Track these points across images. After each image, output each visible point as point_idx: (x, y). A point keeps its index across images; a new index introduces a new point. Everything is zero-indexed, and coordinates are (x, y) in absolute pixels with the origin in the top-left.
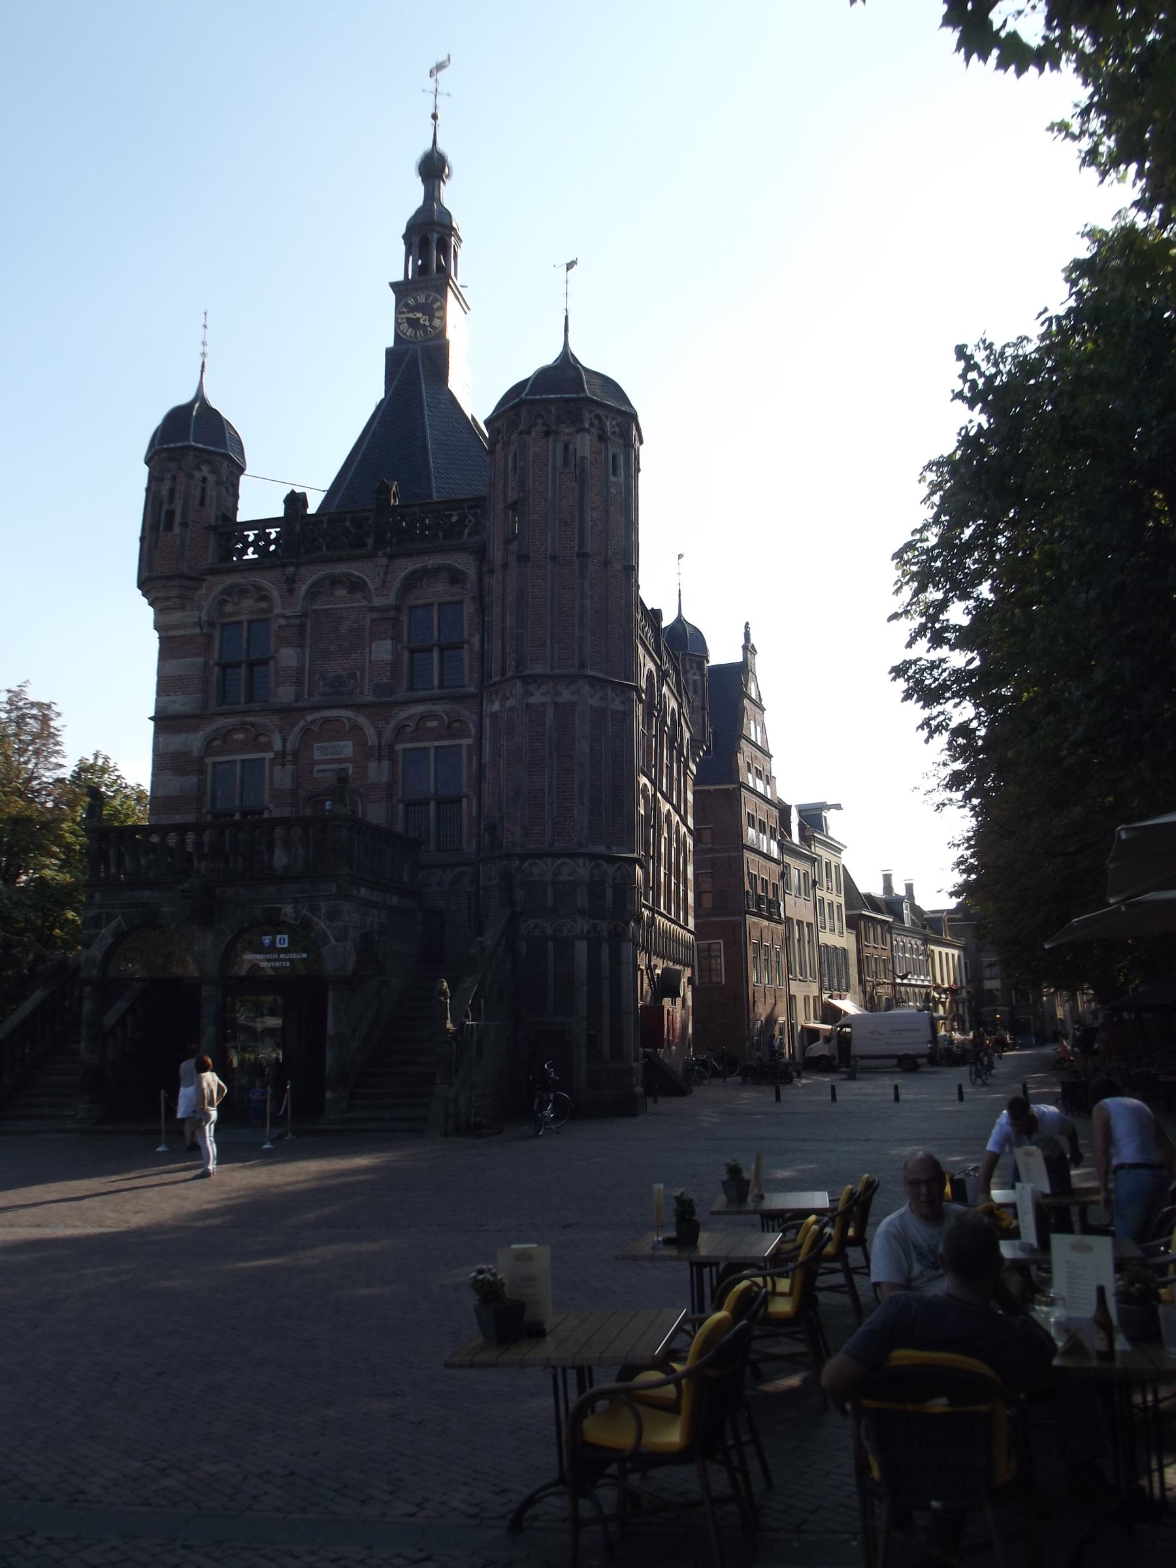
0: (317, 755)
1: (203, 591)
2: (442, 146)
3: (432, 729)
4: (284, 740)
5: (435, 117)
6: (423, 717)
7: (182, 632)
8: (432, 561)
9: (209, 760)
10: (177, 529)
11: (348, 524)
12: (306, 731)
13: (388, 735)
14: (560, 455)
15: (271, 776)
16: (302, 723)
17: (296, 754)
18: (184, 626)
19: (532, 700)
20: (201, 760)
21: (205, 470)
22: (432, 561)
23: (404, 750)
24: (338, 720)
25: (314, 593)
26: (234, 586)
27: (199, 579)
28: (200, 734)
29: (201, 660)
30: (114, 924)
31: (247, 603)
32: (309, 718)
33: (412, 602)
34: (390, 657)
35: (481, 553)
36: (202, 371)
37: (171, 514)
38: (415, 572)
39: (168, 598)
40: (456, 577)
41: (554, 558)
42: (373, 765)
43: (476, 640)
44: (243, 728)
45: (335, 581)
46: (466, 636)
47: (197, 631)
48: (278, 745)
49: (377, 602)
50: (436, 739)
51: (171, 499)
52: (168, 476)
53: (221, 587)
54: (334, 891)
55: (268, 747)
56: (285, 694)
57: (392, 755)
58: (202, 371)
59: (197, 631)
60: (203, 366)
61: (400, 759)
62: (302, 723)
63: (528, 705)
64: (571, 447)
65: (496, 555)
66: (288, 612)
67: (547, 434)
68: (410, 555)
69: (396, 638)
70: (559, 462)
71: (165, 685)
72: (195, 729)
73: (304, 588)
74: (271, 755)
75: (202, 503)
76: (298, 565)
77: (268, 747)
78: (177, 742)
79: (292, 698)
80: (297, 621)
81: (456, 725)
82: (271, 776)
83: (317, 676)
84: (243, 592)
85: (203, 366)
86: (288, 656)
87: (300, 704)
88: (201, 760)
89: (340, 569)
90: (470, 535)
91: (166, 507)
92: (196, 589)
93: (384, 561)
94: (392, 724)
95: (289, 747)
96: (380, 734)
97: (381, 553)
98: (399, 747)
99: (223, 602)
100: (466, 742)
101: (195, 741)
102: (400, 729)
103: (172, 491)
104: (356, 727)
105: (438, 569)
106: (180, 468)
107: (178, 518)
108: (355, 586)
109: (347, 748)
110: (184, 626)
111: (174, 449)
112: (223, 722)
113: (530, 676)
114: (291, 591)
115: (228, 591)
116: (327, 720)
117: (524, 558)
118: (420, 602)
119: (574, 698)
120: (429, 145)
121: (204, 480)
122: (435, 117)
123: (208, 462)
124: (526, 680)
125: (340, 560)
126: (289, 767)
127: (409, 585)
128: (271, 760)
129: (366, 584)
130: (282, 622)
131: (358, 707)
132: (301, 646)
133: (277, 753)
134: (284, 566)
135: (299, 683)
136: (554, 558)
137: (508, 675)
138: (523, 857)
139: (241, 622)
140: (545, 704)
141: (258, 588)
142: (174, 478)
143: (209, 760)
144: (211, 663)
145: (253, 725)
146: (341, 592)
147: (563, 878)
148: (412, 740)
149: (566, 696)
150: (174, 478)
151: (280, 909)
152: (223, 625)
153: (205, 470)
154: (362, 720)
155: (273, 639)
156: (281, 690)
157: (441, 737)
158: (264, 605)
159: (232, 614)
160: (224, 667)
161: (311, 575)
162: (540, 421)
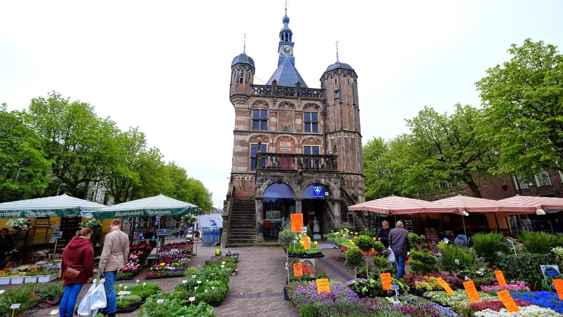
0: (281, 145)
1: (249, 100)
2: (288, 16)
3: (311, 142)
4: (273, 140)
5: (286, 9)
6: (309, 139)
7: (243, 110)
8: (311, 102)
9: (250, 144)
10: (244, 83)
11: (289, 90)
12: (279, 138)
13: (301, 142)
14: (347, 82)
15: (269, 149)
16: (278, 137)
17: (276, 144)
18: (244, 108)
19: (345, 136)
20: (248, 143)
21: (250, 71)
22: (311, 102)
23: (304, 146)
24: (287, 137)
25: (280, 105)
26: (258, 100)
27: (249, 97)
28: (249, 136)
29: (249, 117)
30: (268, 181)
31: (261, 105)
32: (280, 135)
33: (305, 111)
34: (301, 123)
35: (324, 102)
36: (245, 48)
37: (242, 79)
38: (307, 104)
39: (241, 100)
40: (317, 107)
41: (348, 104)
42: (297, 149)
43: (322, 122)
44: (261, 136)
45: (286, 103)
46: (319, 121)
47: (248, 110)
48: (271, 141)
49: (297, 109)
50: (313, 144)
51: (242, 75)
52: (241, 70)
53: (255, 100)
54: (336, 176)
55: (268, 142)
56: (273, 129)
57: (302, 147)
58: (245, 48)
59: (248, 110)
60: (245, 46)
61: (304, 149)
62: (278, 137)
63: (345, 138)
64: (349, 80)
65: (331, 102)
66: (274, 109)
67: (344, 76)
68: (306, 99)
69: (302, 119)
70: (347, 83)
71: (237, 123)
72: (247, 135)
73: (278, 103)
74: (269, 144)
75: (249, 79)
76: (277, 98)
78: (241, 138)
79: (275, 130)
80: (276, 111)
81: (318, 141)
82: (269, 149)
83: (280, 126)
84: (261, 102)
85: (245, 46)
86: (273, 120)
87: (276, 132)
88: (248, 143)
89: (288, 100)
90: (320, 97)
91: (240, 77)
92: (247, 99)
93: (300, 100)
94: (302, 139)
95: (274, 142)
96: (299, 141)
97: (299, 98)
98: (303, 145)
99: (254, 104)
100: (320, 146)
101: (247, 138)
102: (304, 140)
103: (242, 74)
104: (292, 139)
105: (313, 104)
106: (244, 69)
107: (244, 81)
108: (292, 105)
109: (289, 144)
110: (244, 108)
111: (243, 63)
113: (345, 131)
114: (275, 103)
115: (257, 101)
116: (284, 137)
117: (341, 103)
118: (307, 111)
119: (355, 137)
120: (285, 15)
121: (250, 73)
122: (286, 9)
123: (251, 69)
124: (345, 131)
125: (288, 98)
126: (274, 147)
127: (305, 107)
128: (268, 145)
129: (295, 105)
130: (272, 111)
131: (293, 134)
132: (277, 117)
133: (270, 143)
134: (273, 97)
135: (276, 127)
136: (348, 104)
137: (337, 130)
138: (347, 174)
139: (259, 110)
140: (348, 138)
142: (242, 71)
143: (250, 144)
144: (251, 119)
145: (264, 136)
146: (286, 106)
147: (355, 180)
148: (306, 144)
149: (353, 137)
150: (242, 71)
151: (320, 180)
152: (254, 110)
153: (250, 71)
154: (294, 137)
155: (268, 115)
156: (272, 128)
157: (313, 144)
158: (266, 106)
159: (256, 107)
160: (254, 120)
161: (280, 101)
162: (343, 73)
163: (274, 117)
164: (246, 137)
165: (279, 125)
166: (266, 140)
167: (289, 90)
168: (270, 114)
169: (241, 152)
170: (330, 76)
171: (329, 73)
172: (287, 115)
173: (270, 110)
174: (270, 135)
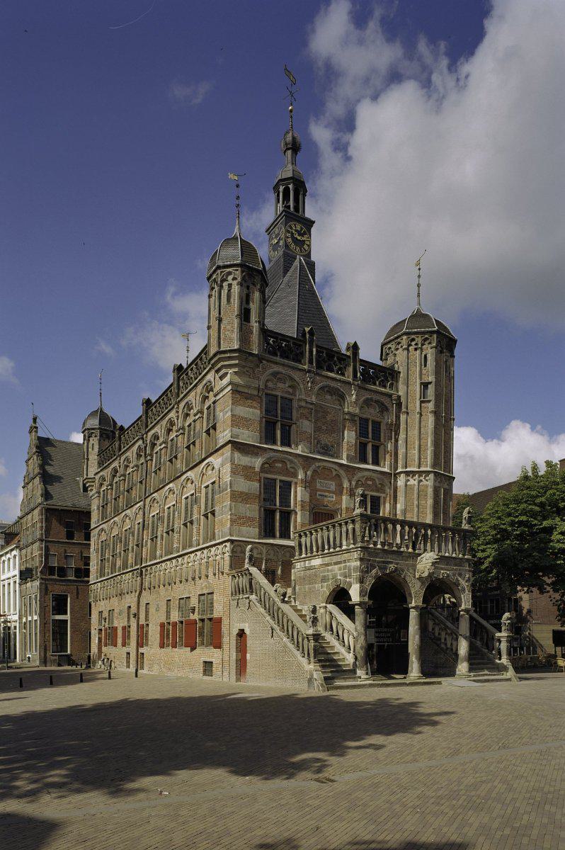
11: (335, 359)
31: (280, 385)
66: (308, 399)
77: (295, 475)
101: (257, 462)
112: (272, 454)
130: (303, 404)
141: (292, 379)
143: (263, 475)
146: (328, 397)
158: (291, 390)
163: (307, 418)
164: (253, 460)
165: (315, 439)
166: (293, 470)
167: (335, 359)
168: (298, 411)
169: (247, 494)
170: (413, 343)
171: (413, 336)
172: (329, 418)
173: (300, 400)
174: (301, 460)
